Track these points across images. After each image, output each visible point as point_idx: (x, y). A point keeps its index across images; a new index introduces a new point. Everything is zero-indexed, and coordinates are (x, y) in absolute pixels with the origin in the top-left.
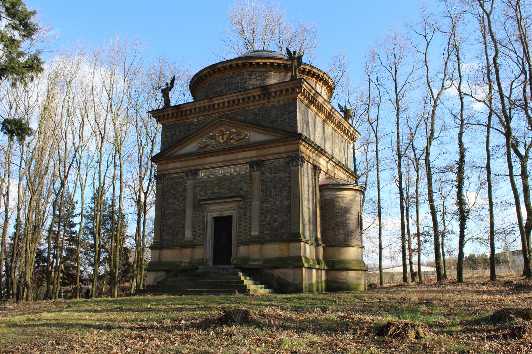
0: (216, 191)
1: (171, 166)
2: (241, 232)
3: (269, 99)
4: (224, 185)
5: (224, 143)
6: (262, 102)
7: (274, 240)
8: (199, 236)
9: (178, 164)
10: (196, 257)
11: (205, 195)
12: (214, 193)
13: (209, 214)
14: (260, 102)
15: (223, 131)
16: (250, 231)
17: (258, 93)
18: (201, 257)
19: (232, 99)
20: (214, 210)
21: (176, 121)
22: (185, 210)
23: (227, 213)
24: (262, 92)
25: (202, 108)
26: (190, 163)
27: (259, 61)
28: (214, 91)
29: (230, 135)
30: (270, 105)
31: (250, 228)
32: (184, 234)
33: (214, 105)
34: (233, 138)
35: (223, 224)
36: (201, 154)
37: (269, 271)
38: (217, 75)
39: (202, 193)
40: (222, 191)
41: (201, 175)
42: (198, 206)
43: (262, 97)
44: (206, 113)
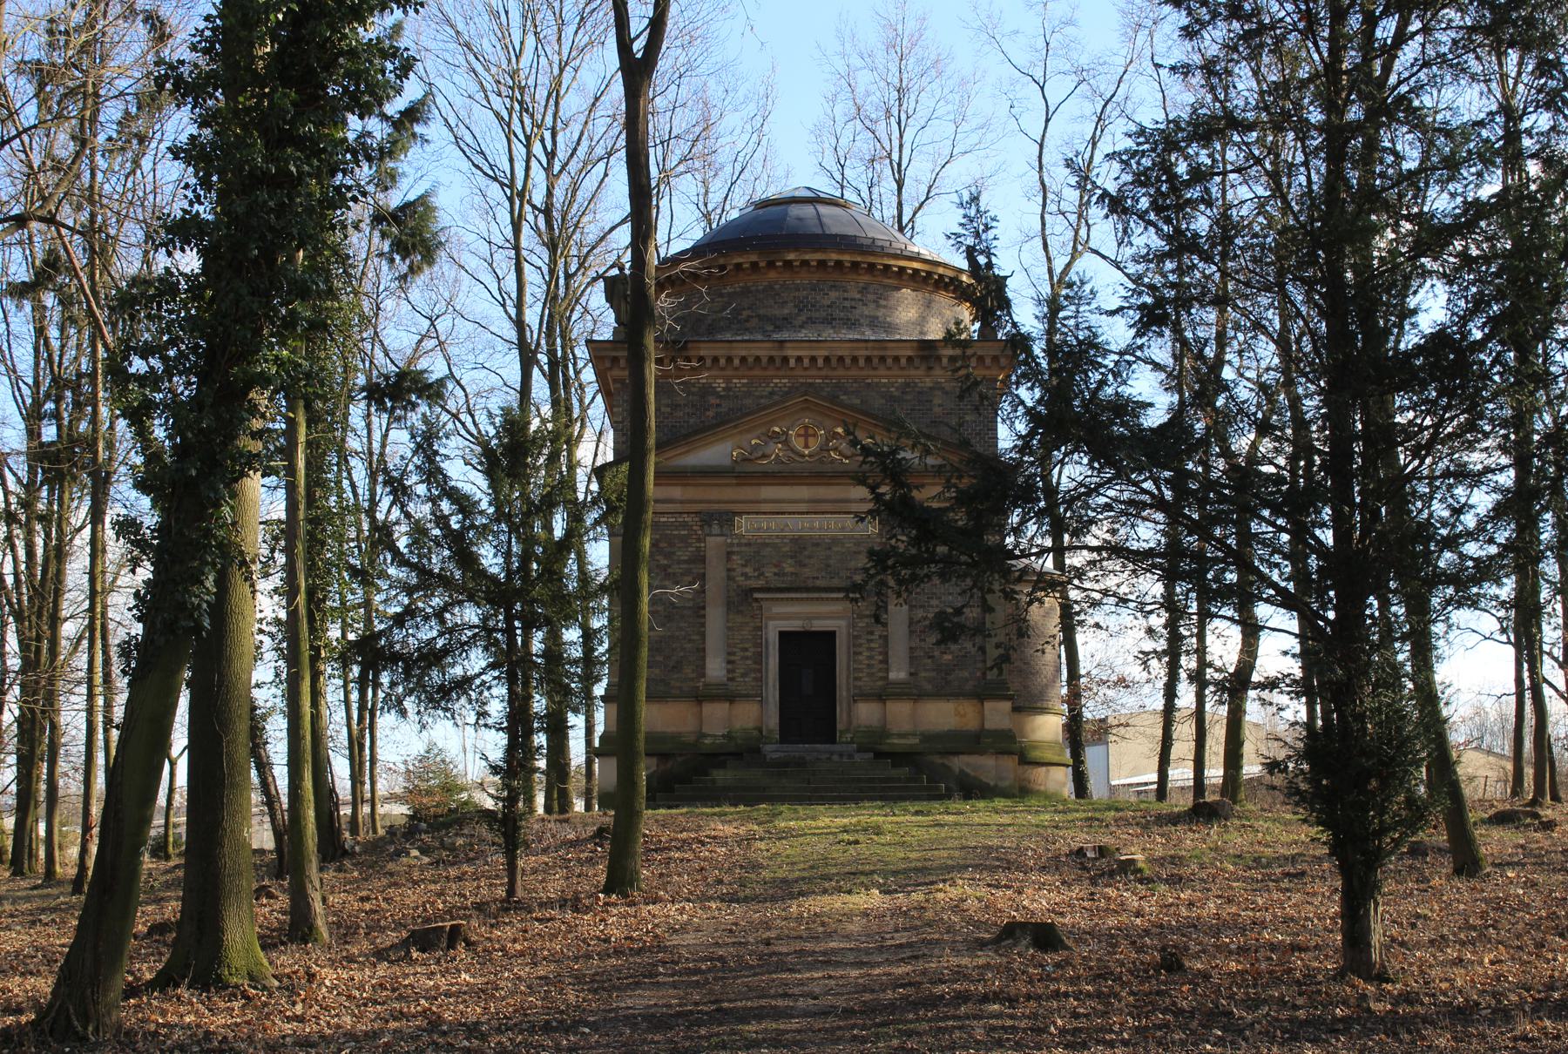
0: (788, 569)
2: (860, 670)
4: (810, 557)
6: (913, 372)
7: (943, 691)
8: (743, 675)
10: (738, 725)
11: (758, 578)
12: (784, 574)
13: (771, 624)
15: (806, 428)
16: (887, 671)
17: (910, 353)
18: (751, 725)
19: (840, 353)
20: (786, 616)
22: (704, 608)
23: (819, 625)
25: (751, 360)
26: (714, 493)
27: (892, 262)
28: (761, 312)
29: (828, 441)
30: (928, 382)
31: (885, 661)
32: (703, 667)
33: (785, 359)
37: (938, 760)
38: (772, 275)
39: (748, 570)
40: (807, 572)
41: (743, 525)
42: (743, 600)
43: (917, 362)
44: (757, 372)
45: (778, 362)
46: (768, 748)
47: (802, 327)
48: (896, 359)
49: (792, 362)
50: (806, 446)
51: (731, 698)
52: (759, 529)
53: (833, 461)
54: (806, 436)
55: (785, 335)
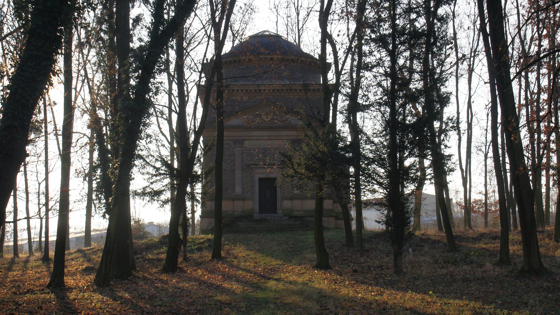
5: (268, 121)
13: (256, 175)
17: (300, 88)
23: (272, 176)
33: (260, 90)
35: (268, 185)
39: (248, 158)
41: (246, 144)
45: (258, 91)
46: (255, 215)
47: (265, 79)
48: (296, 90)
49: (262, 91)
50: (267, 118)
51: (244, 199)
53: (276, 123)
55: (260, 82)
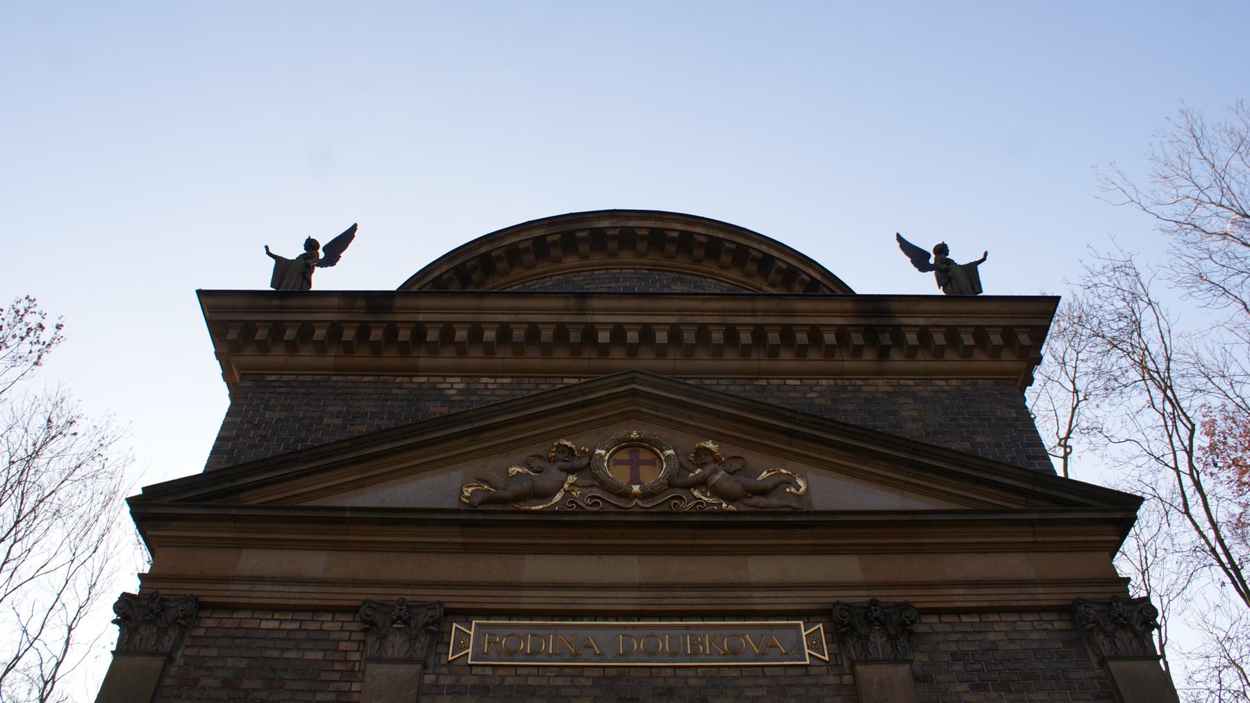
1: (252, 561)
3: (883, 354)
5: (646, 495)
9: (315, 563)
14: (835, 365)
21: (338, 370)
24: (861, 321)
34: (701, 483)
36: (495, 523)
50: (635, 479)
52: (511, 654)
54: (635, 465)
